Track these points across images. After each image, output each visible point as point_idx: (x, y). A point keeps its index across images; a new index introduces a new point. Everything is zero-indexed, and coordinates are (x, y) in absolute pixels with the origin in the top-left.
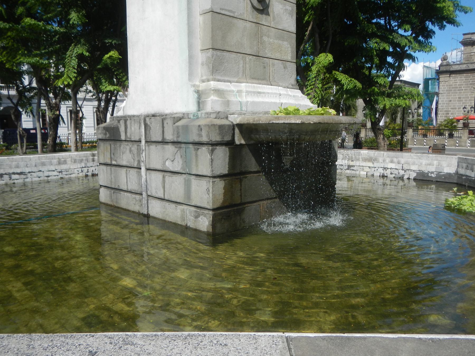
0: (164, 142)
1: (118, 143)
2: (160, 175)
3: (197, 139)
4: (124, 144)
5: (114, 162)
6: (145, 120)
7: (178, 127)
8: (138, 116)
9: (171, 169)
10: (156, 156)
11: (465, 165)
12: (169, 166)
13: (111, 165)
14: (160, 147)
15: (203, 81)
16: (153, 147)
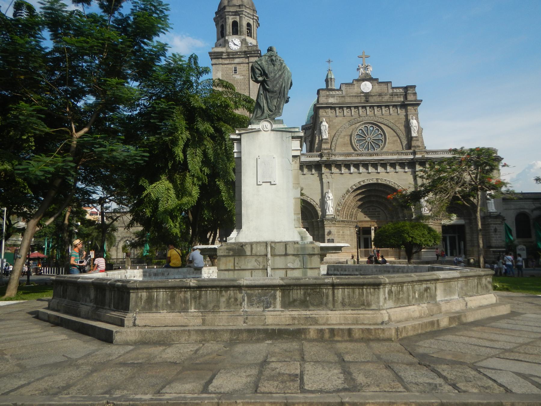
0: (286, 255)
1: (243, 258)
2: (284, 271)
3: (311, 253)
4: (248, 258)
5: (236, 268)
6: (271, 245)
7: (298, 248)
8: (266, 243)
9: (292, 267)
10: (280, 262)
11: (333, 269)
12: (290, 265)
13: (235, 270)
14: (283, 258)
15: (296, 228)
16: (277, 258)
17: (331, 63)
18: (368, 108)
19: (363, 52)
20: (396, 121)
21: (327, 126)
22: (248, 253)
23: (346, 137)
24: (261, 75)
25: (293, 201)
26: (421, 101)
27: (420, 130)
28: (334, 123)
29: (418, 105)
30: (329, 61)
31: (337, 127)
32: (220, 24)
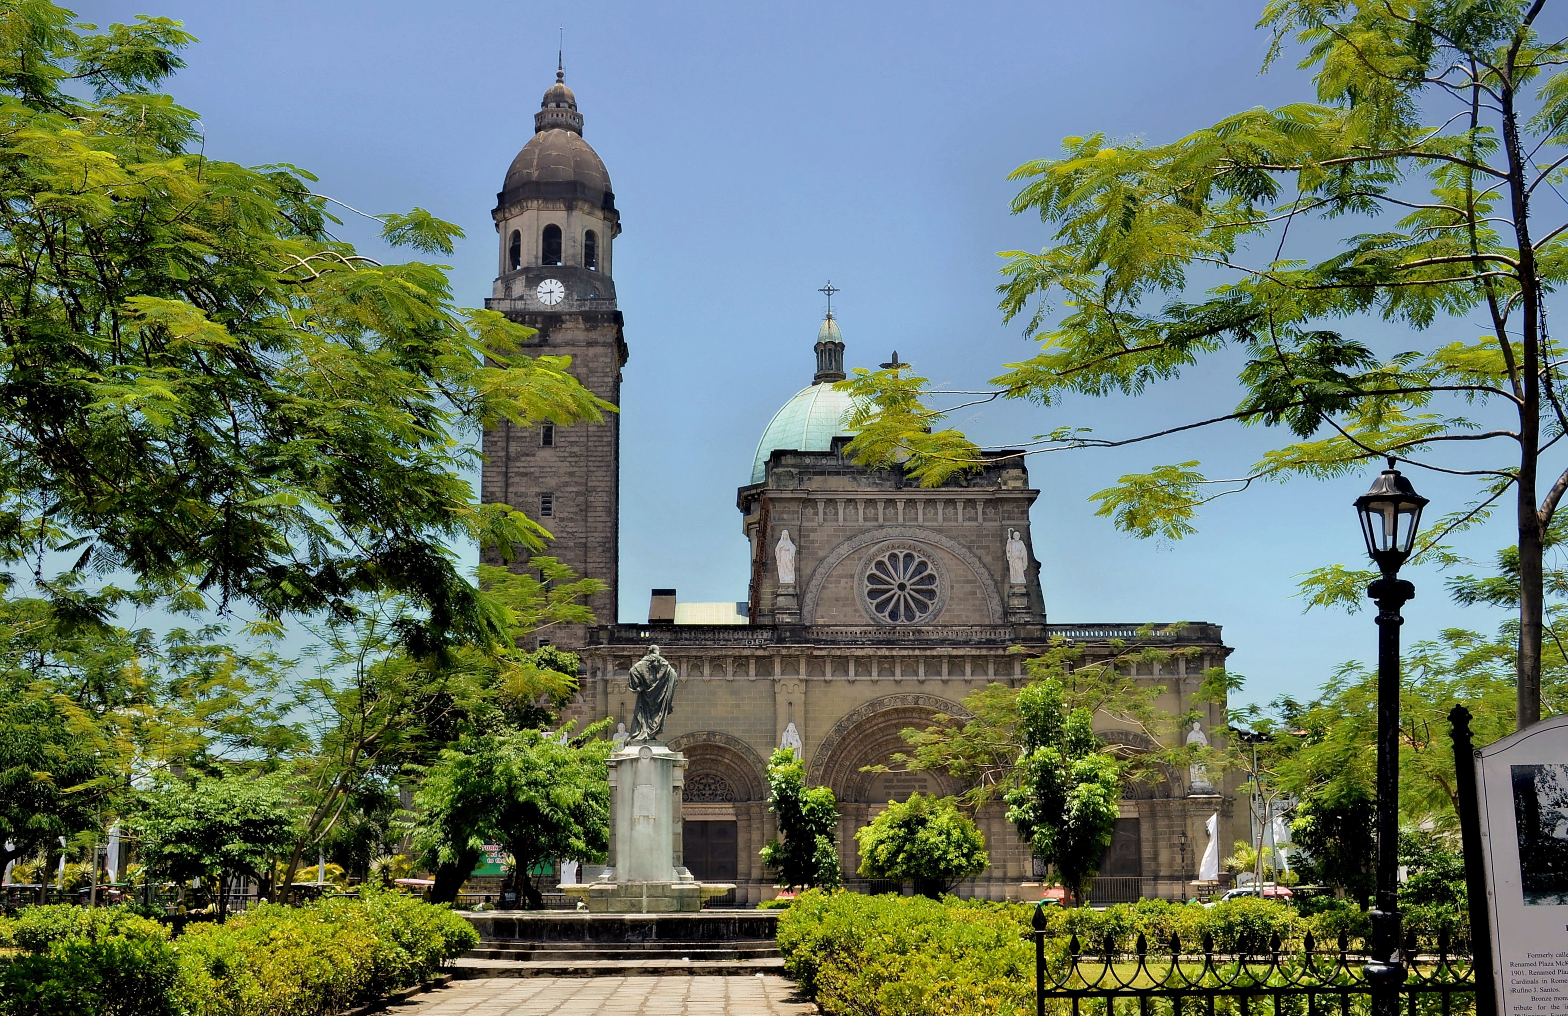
17: (834, 296)
18: (900, 506)
19: (895, 356)
20: (972, 542)
21: (793, 548)
22: (622, 893)
23: (843, 581)
24: (640, 685)
25: (670, 838)
26: (1038, 492)
27: (1034, 566)
28: (813, 542)
29: (1031, 501)
30: (829, 291)
31: (821, 554)
32: (510, 232)
